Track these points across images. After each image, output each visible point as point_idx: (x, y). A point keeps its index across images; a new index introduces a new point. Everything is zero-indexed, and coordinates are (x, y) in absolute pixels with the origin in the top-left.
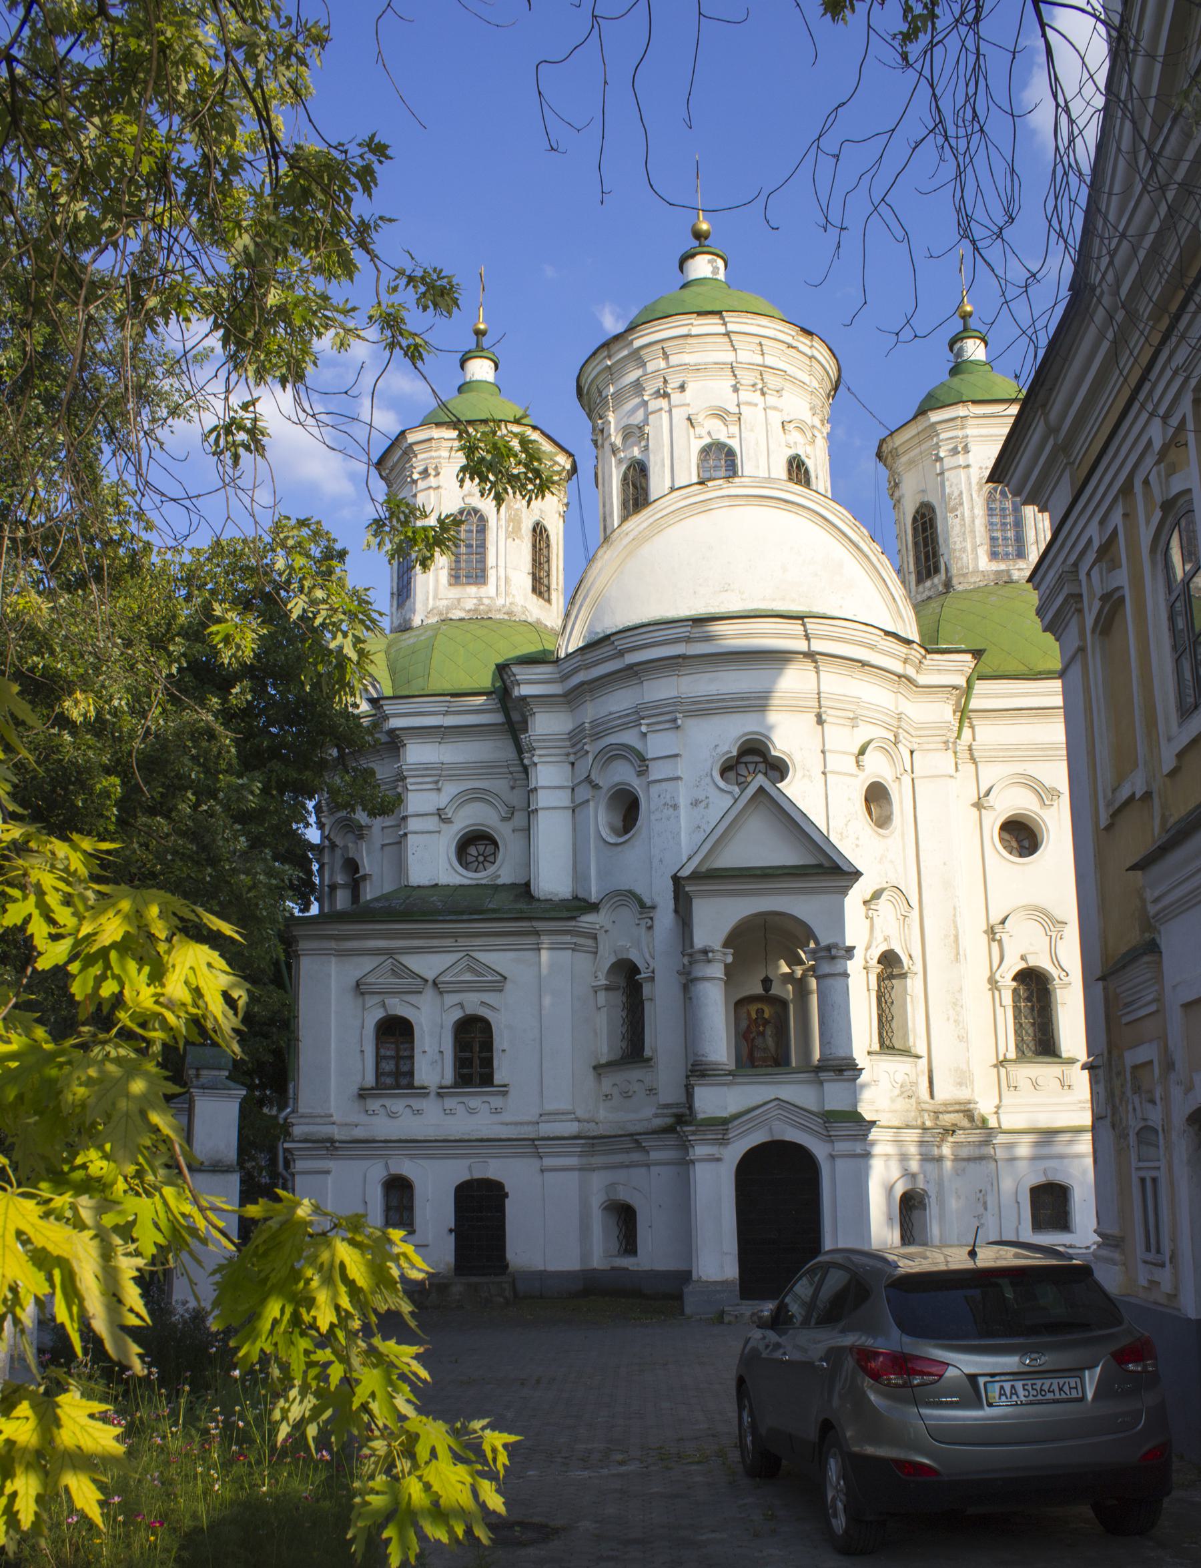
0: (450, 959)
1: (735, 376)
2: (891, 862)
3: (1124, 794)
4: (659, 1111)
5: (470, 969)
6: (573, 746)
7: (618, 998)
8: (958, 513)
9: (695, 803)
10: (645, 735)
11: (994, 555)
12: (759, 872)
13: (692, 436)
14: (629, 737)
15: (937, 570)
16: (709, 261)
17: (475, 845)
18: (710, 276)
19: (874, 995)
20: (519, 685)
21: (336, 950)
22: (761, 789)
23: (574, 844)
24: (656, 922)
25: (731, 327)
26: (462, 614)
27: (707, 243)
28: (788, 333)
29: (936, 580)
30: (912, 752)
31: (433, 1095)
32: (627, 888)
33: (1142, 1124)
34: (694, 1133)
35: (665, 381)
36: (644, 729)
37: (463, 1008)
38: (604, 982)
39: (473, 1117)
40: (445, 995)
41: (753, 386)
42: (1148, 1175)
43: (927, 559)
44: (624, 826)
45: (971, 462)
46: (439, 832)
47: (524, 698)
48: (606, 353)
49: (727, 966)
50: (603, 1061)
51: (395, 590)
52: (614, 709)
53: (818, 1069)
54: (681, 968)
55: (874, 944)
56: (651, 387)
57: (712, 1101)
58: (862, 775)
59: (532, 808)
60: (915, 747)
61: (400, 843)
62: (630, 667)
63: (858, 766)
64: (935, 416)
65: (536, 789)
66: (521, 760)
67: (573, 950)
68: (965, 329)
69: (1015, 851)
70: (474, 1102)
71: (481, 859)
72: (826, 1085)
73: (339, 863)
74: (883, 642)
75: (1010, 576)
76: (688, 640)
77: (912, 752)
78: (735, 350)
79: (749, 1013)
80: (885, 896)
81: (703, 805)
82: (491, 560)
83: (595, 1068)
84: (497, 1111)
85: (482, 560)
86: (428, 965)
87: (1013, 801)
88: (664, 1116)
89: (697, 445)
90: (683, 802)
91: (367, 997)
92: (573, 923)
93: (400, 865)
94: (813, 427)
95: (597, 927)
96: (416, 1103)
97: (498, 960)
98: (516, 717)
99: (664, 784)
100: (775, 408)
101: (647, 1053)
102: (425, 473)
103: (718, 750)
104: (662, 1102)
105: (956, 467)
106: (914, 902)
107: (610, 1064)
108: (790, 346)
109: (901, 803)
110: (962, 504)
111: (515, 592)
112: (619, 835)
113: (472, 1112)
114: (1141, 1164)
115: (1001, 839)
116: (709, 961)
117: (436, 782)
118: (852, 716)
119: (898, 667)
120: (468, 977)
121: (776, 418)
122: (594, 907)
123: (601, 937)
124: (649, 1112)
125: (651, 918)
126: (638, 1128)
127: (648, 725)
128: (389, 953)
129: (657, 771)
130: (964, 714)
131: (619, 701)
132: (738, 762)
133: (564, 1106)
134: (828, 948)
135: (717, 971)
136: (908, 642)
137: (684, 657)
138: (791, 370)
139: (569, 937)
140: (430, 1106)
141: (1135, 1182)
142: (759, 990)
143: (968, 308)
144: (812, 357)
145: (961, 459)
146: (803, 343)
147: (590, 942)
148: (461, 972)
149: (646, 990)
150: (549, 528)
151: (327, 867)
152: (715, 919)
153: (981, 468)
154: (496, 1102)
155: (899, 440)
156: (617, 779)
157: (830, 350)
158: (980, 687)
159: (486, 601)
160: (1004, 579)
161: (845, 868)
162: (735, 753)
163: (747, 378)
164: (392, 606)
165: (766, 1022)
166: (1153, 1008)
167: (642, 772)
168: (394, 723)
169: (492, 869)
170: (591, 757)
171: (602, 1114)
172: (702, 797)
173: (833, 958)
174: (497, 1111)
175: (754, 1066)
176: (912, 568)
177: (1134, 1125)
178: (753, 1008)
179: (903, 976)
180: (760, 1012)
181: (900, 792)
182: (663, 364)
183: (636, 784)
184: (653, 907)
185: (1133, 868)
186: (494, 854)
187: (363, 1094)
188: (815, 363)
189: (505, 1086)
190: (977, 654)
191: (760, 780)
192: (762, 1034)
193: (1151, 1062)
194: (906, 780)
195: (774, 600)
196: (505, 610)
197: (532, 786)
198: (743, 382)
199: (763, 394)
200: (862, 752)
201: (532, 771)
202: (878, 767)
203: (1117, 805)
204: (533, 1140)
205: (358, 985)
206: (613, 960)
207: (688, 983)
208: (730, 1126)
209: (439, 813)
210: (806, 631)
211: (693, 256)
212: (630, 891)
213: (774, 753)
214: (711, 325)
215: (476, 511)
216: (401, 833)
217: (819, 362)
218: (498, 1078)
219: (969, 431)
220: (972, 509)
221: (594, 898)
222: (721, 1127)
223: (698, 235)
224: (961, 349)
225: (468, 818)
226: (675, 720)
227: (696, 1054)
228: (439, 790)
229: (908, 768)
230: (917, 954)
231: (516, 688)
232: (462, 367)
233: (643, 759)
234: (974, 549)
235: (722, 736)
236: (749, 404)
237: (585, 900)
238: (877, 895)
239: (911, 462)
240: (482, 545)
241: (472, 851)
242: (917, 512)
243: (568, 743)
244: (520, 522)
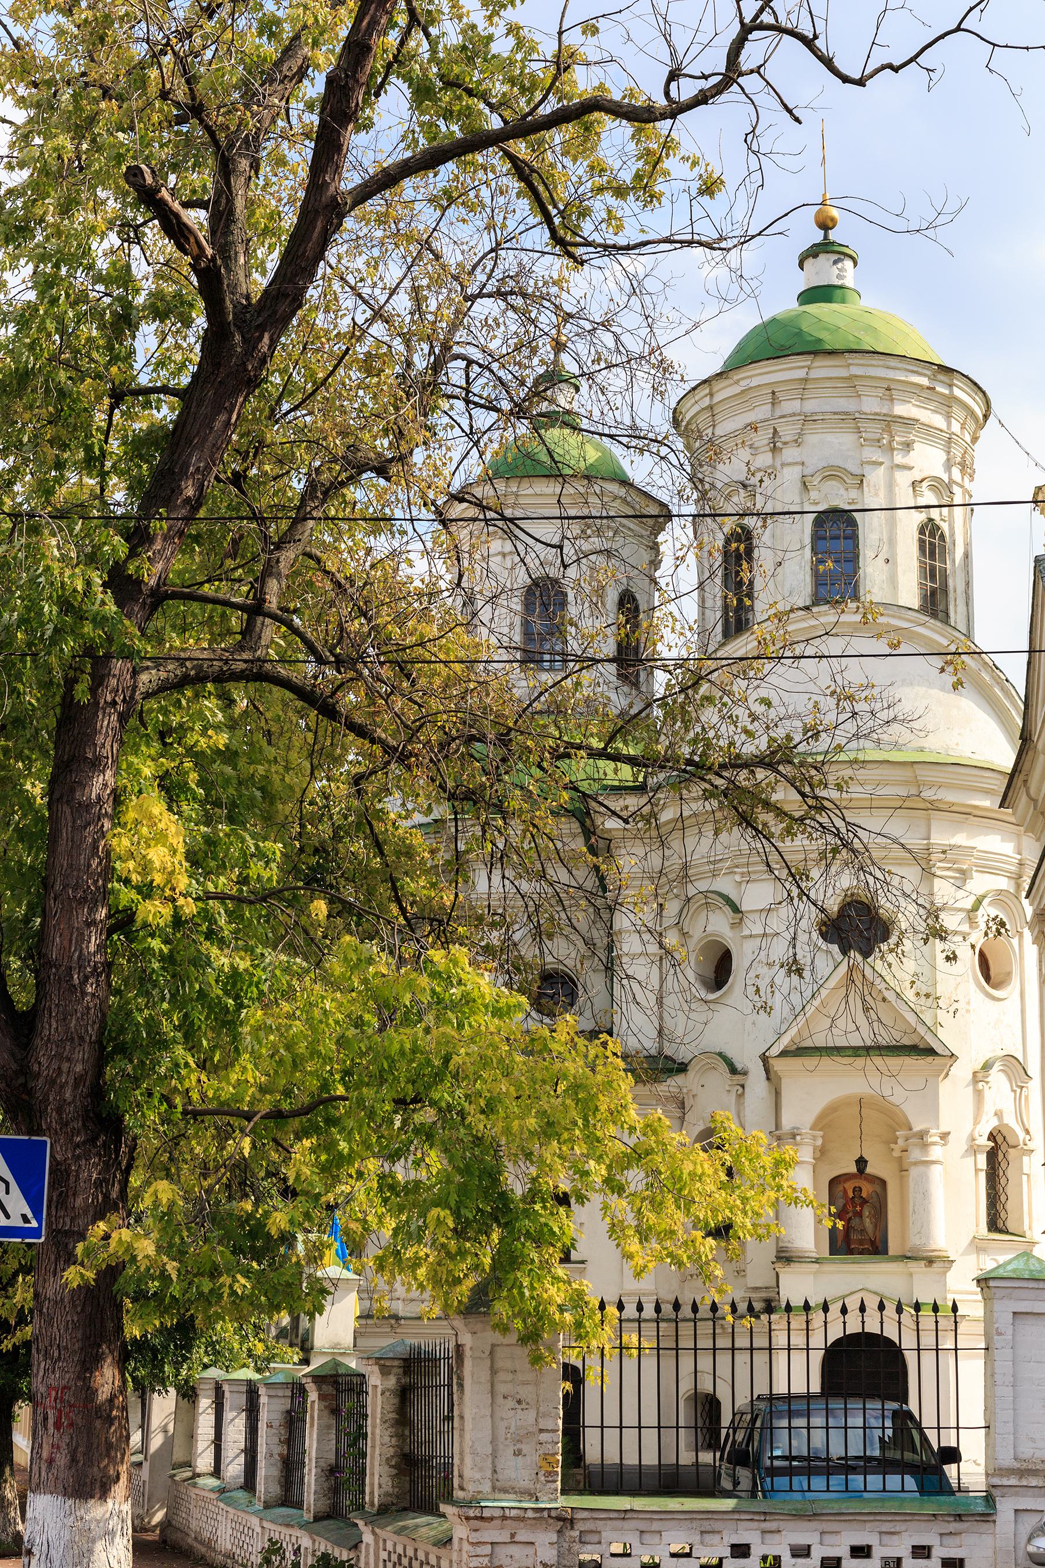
14: (724, 885)
19: (983, 1176)
36: (738, 878)
48: (707, 391)
57: (796, 1286)
79: (845, 1191)
122: (682, 1068)
125: (743, 1086)
135: (806, 1154)
165: (864, 1202)
178: (849, 1186)
184: (745, 1073)
189: (583, 1262)
192: (860, 1215)
212: (720, 1054)
233: (736, 909)
238: (987, 1066)
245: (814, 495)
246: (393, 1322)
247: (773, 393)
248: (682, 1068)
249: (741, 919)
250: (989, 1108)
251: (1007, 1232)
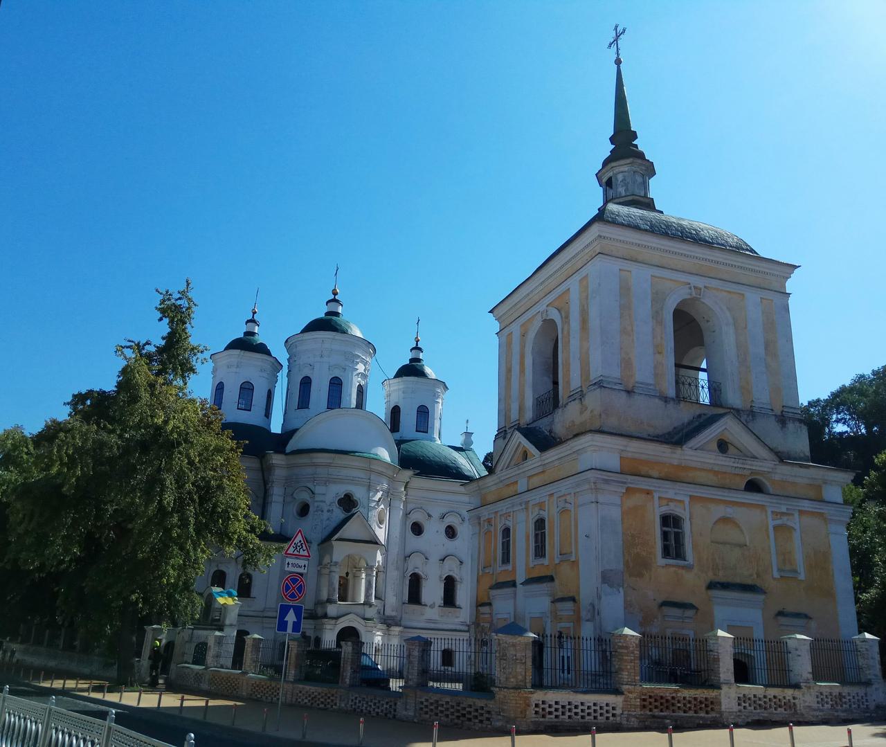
9: (329, 511)
15: (398, 431)
87: (416, 517)
99: (319, 504)
129: (318, 498)
183: (310, 501)
233: (313, 493)
245: (331, 372)
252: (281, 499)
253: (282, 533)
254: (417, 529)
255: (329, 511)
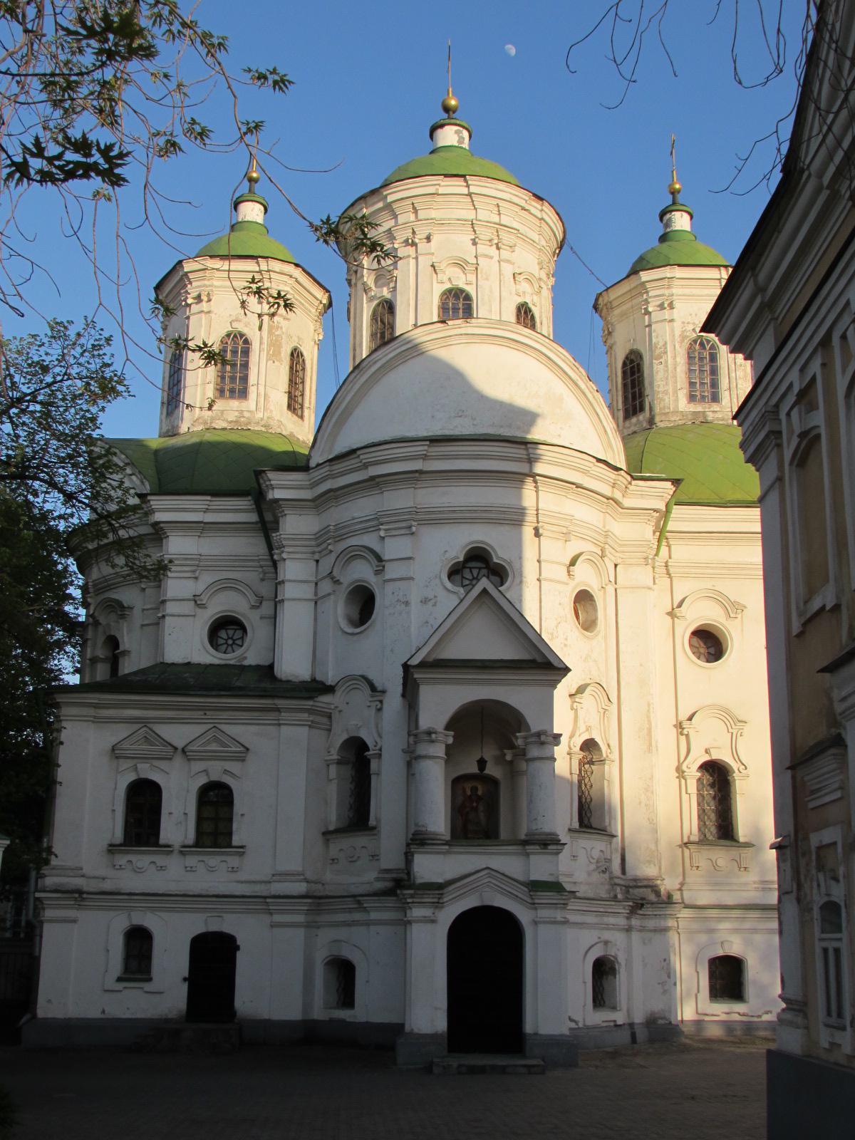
0: (197, 730)
1: (474, 231)
2: (595, 661)
3: (816, 605)
4: (380, 875)
5: (216, 739)
6: (318, 545)
7: (348, 771)
8: (662, 360)
9: (425, 601)
10: (383, 538)
11: (692, 398)
12: (479, 664)
13: (435, 281)
14: (369, 540)
15: (642, 409)
16: (457, 132)
17: (225, 629)
18: (457, 145)
20: (273, 489)
21: (95, 717)
22: (485, 591)
23: (315, 633)
24: (385, 706)
25: (473, 189)
26: (224, 425)
27: (454, 116)
28: (522, 197)
29: (641, 417)
30: (616, 566)
31: (176, 852)
32: (360, 673)
33: (826, 899)
34: (412, 896)
35: (414, 232)
36: (382, 533)
37: (207, 775)
38: (335, 757)
39: (211, 874)
40: (193, 762)
41: (490, 241)
42: (831, 945)
43: (634, 398)
44: (360, 619)
45: (675, 317)
46: (194, 616)
47: (277, 501)
49: (448, 747)
50: (332, 828)
51: (165, 400)
52: (356, 515)
53: (525, 843)
54: (405, 747)
55: (577, 734)
56: (401, 236)
57: (428, 867)
58: (572, 583)
59: (279, 598)
60: (619, 561)
61: (158, 624)
62: (372, 478)
63: (569, 575)
64: (645, 276)
65: (283, 582)
66: (272, 555)
67: (310, 726)
68: (674, 203)
69: (702, 657)
70: (213, 861)
71: (230, 642)
72: (531, 857)
73: (101, 640)
74: (594, 468)
75: (705, 417)
76: (425, 457)
77: (616, 566)
78: (476, 209)
79: (464, 790)
80: (588, 690)
81: (430, 604)
82: (252, 379)
83: (324, 834)
84: (233, 870)
85: (245, 379)
86: (179, 734)
87: (701, 613)
88: (384, 879)
89: (438, 290)
90: (415, 599)
91: (121, 761)
92: (311, 703)
93: (158, 644)
94: (540, 279)
95: (332, 707)
96: (160, 860)
97: (244, 732)
98: (268, 517)
99: (398, 583)
100: (508, 261)
101: (372, 822)
102: (198, 299)
103: (447, 555)
104: (385, 866)
105: (662, 321)
106: (614, 698)
107: (337, 831)
108: (523, 209)
109: (605, 609)
110: (665, 353)
111: (272, 408)
112: (357, 626)
113: (211, 870)
114: (824, 936)
115: (691, 645)
116: (433, 741)
117: (194, 572)
118: (564, 530)
119: (607, 491)
120: (214, 747)
121: (508, 270)
122: (330, 689)
123: (335, 716)
124: (372, 875)
125: (381, 702)
126: (361, 890)
127: (386, 530)
128: (144, 722)
129: (392, 571)
130: (661, 533)
131: (361, 508)
132: (464, 567)
133: (295, 866)
134: (539, 734)
135: (439, 750)
136: (617, 469)
137: (420, 472)
138: (522, 229)
139: (306, 715)
140: (174, 865)
141: (818, 951)
142: (474, 769)
143: (677, 186)
144: (542, 219)
145: (666, 314)
146: (535, 206)
147: (325, 720)
148: (208, 742)
149: (374, 765)
150: (305, 353)
151: (89, 643)
152: (441, 702)
153: (683, 323)
154: (233, 861)
155: (613, 294)
156: (356, 576)
157: (558, 214)
158: (677, 511)
159: (246, 414)
160: (701, 419)
161: (556, 664)
162: (461, 559)
163: (484, 233)
164: (161, 413)
165: (479, 799)
166: (838, 795)
167: (379, 572)
168: (159, 517)
169: (239, 652)
170: (333, 556)
171: (328, 876)
172: (431, 596)
173: (543, 743)
174: (233, 870)
175: (466, 838)
176: (620, 406)
177: (818, 900)
178: (468, 786)
179: (602, 761)
180: (474, 789)
181: (605, 600)
182: (412, 217)
183: (372, 580)
184: (384, 692)
185: (823, 670)
186: (242, 638)
187: (112, 849)
188: (544, 225)
190: (676, 482)
191: (484, 583)
192: (476, 809)
193: (835, 844)
194: (610, 589)
195: (502, 427)
196: (263, 423)
197: (280, 579)
198: (481, 237)
199: (498, 248)
200: (573, 562)
201: (280, 566)
202: (585, 577)
203: (808, 616)
204: (265, 897)
205: (113, 749)
206: (345, 737)
207: (412, 759)
208: (445, 890)
209: (196, 600)
210: (528, 455)
211: (442, 126)
212: (363, 677)
213: (495, 560)
214: (456, 186)
215: (242, 335)
216: (160, 615)
217: (547, 224)
218: (236, 840)
219: (674, 291)
220: (674, 358)
221: (330, 682)
222: (437, 890)
223: (447, 109)
224: (670, 219)
225: (218, 606)
226: (410, 527)
227: (416, 825)
228: (196, 578)
229: (612, 579)
230: (614, 744)
231: (270, 492)
232: (236, 208)
234: (675, 392)
235: (452, 543)
236: (486, 256)
237: (322, 683)
238: (581, 690)
239: (624, 315)
240: (245, 366)
241: (223, 634)
242: (627, 358)
243: (313, 543)
244: (280, 346)
246: (77, 895)
247: (413, 204)
248: (330, 689)
249: (384, 567)
250: (582, 727)
251: (591, 827)
252: (307, 591)
253: (319, 678)
254: (710, 643)
255: (425, 601)
